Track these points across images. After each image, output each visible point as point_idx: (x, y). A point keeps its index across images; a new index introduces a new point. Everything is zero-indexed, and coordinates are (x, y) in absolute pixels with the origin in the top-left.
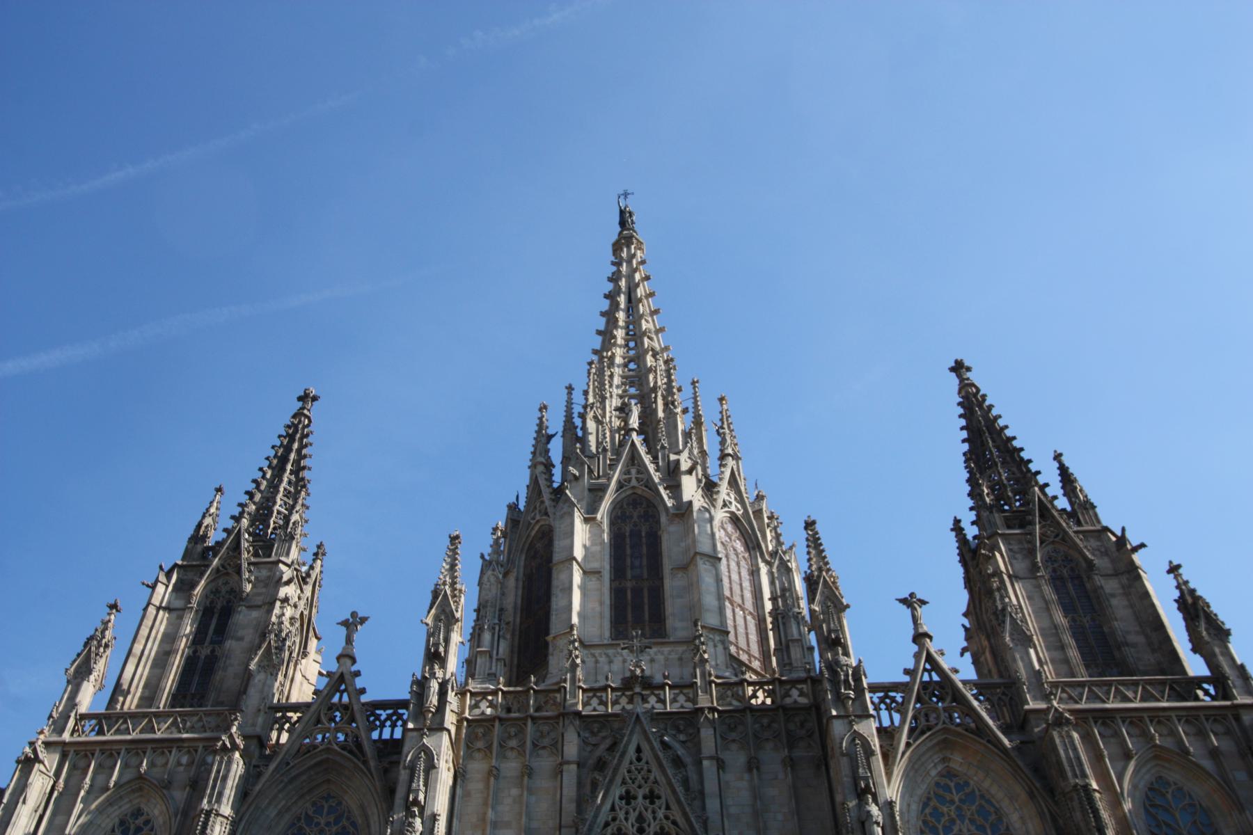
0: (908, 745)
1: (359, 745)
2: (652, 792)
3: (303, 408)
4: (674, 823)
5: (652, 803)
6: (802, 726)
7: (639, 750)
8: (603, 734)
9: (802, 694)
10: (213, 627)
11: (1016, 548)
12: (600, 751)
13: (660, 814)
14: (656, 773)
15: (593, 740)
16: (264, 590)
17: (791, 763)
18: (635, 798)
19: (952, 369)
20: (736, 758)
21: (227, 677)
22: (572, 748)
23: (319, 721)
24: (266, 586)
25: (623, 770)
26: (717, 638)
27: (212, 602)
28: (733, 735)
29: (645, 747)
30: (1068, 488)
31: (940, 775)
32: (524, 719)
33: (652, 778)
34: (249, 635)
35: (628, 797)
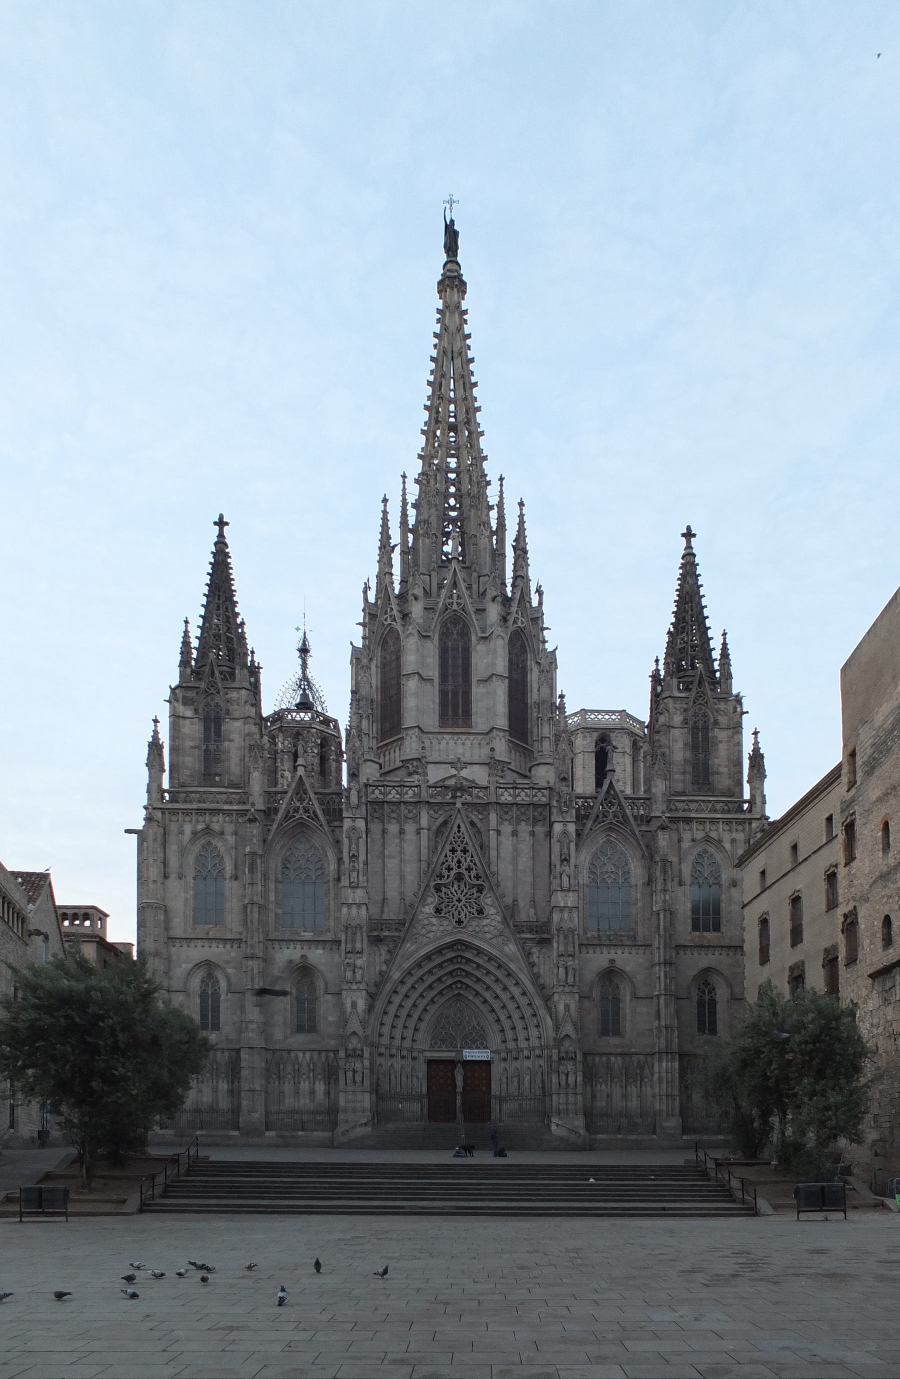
0: (591, 829)
1: (316, 816)
2: (465, 848)
3: (221, 535)
4: (475, 864)
6: (541, 814)
7: (459, 827)
8: (440, 812)
9: (544, 796)
11: (678, 706)
13: (468, 860)
14: (467, 839)
15: (436, 816)
19: (683, 535)
22: (424, 822)
23: (292, 800)
26: (501, 734)
28: (506, 817)
29: (462, 826)
30: (723, 661)
32: (400, 802)
35: (453, 851)
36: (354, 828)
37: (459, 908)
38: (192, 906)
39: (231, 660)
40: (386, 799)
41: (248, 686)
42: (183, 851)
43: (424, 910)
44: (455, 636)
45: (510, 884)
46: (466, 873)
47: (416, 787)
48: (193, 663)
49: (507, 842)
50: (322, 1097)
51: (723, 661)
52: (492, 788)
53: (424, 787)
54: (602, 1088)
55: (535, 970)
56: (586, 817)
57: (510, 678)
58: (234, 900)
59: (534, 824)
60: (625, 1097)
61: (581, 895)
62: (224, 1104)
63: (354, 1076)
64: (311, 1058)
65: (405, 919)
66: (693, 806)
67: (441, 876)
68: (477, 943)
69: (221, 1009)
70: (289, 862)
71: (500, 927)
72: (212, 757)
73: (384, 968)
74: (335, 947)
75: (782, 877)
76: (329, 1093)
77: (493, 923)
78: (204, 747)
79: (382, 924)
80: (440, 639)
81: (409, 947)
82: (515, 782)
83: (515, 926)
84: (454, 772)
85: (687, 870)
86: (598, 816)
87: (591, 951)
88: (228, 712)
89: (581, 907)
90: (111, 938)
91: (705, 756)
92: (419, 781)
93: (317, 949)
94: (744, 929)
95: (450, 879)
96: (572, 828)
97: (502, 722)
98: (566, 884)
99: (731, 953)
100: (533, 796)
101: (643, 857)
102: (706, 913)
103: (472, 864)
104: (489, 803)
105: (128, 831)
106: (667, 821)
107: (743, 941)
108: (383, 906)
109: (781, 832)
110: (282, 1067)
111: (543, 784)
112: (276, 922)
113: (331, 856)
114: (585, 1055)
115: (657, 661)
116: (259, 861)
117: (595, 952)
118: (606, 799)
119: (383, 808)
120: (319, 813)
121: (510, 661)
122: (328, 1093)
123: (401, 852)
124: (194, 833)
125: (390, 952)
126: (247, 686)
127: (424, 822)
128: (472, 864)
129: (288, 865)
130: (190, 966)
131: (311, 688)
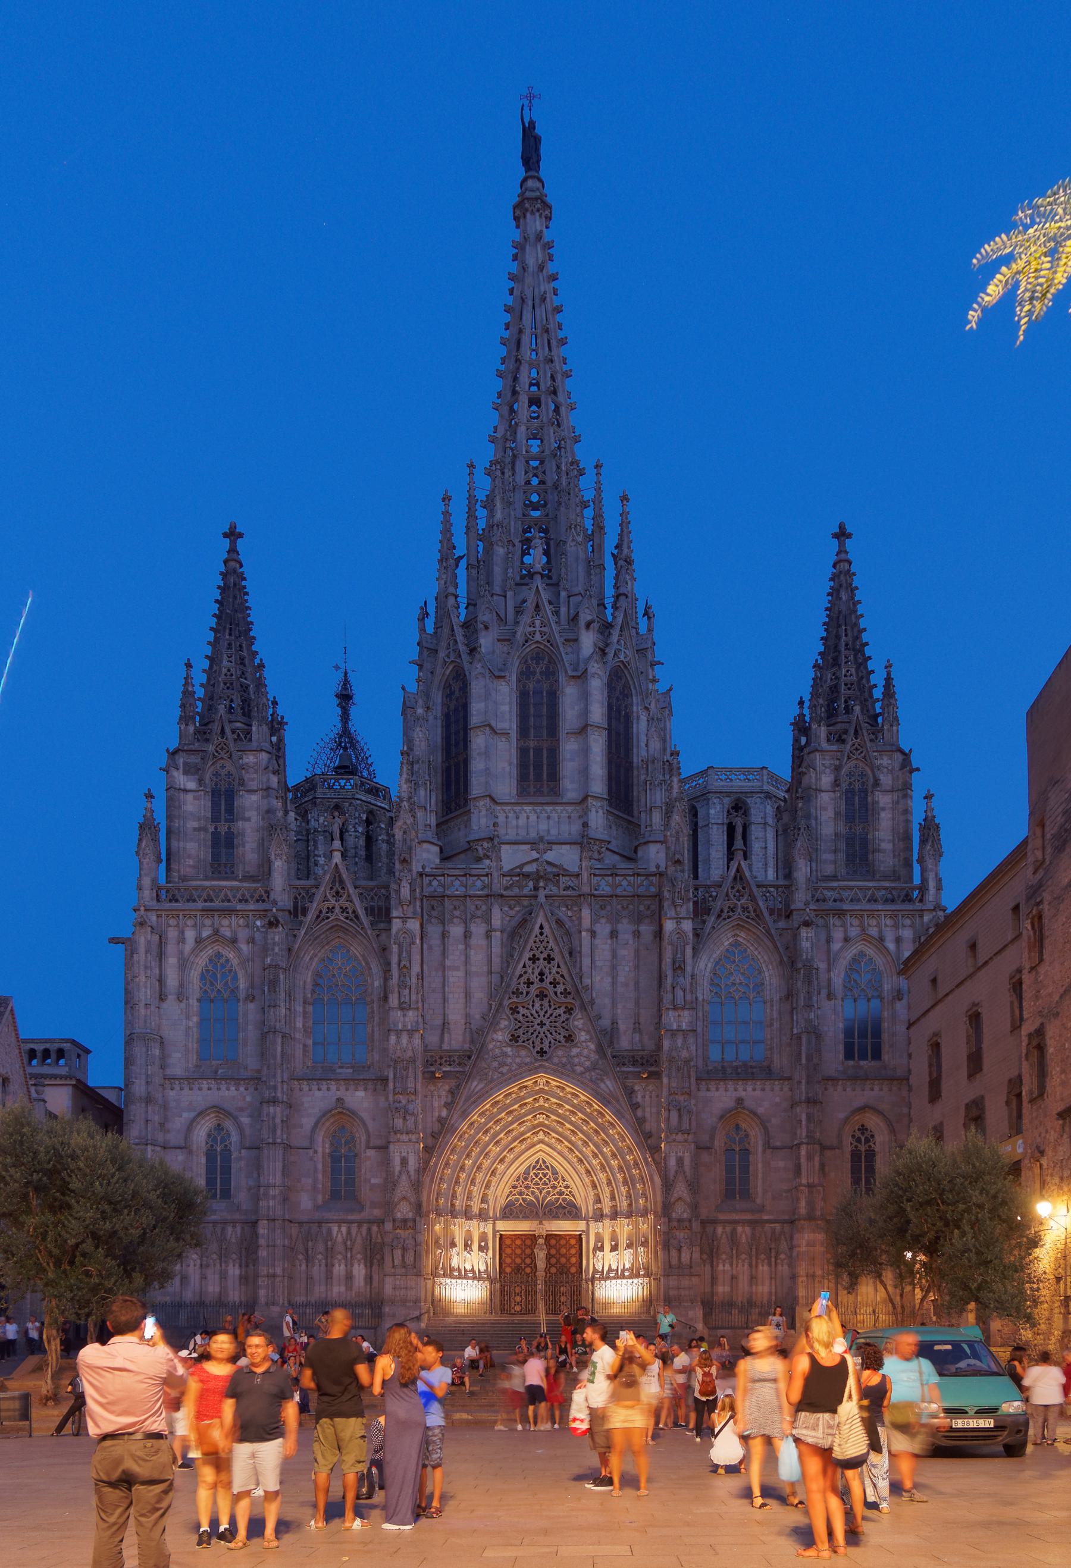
1: (357, 917)
2: (549, 956)
4: (562, 976)
5: (549, 963)
7: (541, 927)
8: (517, 909)
10: (223, 807)
12: (514, 923)
13: (554, 970)
14: (552, 944)
16: (255, 776)
17: (637, 934)
18: (538, 959)
20: (603, 929)
21: (248, 851)
24: (256, 772)
25: (531, 941)
27: (216, 785)
28: (603, 912)
31: (731, 945)
32: (466, 896)
34: (253, 814)
35: (534, 959)
36: (406, 932)
37: (542, 1035)
38: (195, 1037)
39: (247, 714)
40: (448, 893)
41: (269, 749)
42: (184, 965)
43: (495, 1036)
44: (538, 676)
45: (607, 1001)
46: (550, 988)
47: (487, 875)
48: (198, 718)
49: (604, 947)
50: (362, 1283)
51: (886, 702)
52: (585, 875)
53: (495, 874)
54: (723, 1267)
56: (708, 911)
57: (609, 730)
58: (250, 1027)
59: (639, 921)
60: (753, 1278)
61: (700, 1014)
62: (235, 1295)
63: (403, 1256)
64: (349, 1233)
65: (471, 1050)
66: (845, 894)
67: (517, 993)
69: (233, 1171)
70: (321, 977)
71: (594, 1057)
72: (223, 845)
73: (444, 1113)
74: (379, 1087)
75: (958, 986)
76: (371, 1278)
78: (211, 829)
79: (441, 1058)
80: (519, 681)
82: (614, 867)
83: (614, 1057)
84: (535, 855)
85: (838, 978)
86: (722, 911)
87: (712, 1087)
88: (243, 785)
89: (699, 1030)
90: (93, 1081)
91: (863, 828)
92: (490, 867)
94: (910, 1056)
95: (530, 996)
96: (687, 926)
97: (598, 786)
98: (679, 1000)
99: (894, 1088)
100: (638, 887)
101: (781, 962)
102: (863, 1035)
103: (558, 977)
104: (580, 896)
105: (114, 941)
106: (813, 914)
107: (909, 1071)
108: (442, 1034)
109: (957, 926)
110: (310, 1244)
111: (653, 869)
112: (304, 1055)
113: (376, 968)
114: (703, 1223)
115: (801, 703)
116: (282, 977)
117: (717, 1089)
118: (733, 888)
120: (361, 912)
121: (610, 707)
122: (369, 1278)
123: (467, 961)
124: (199, 941)
125: (452, 1093)
126: (269, 749)
127: (497, 921)
128: (558, 977)
129: (320, 981)
130: (192, 1115)
131: (354, 748)
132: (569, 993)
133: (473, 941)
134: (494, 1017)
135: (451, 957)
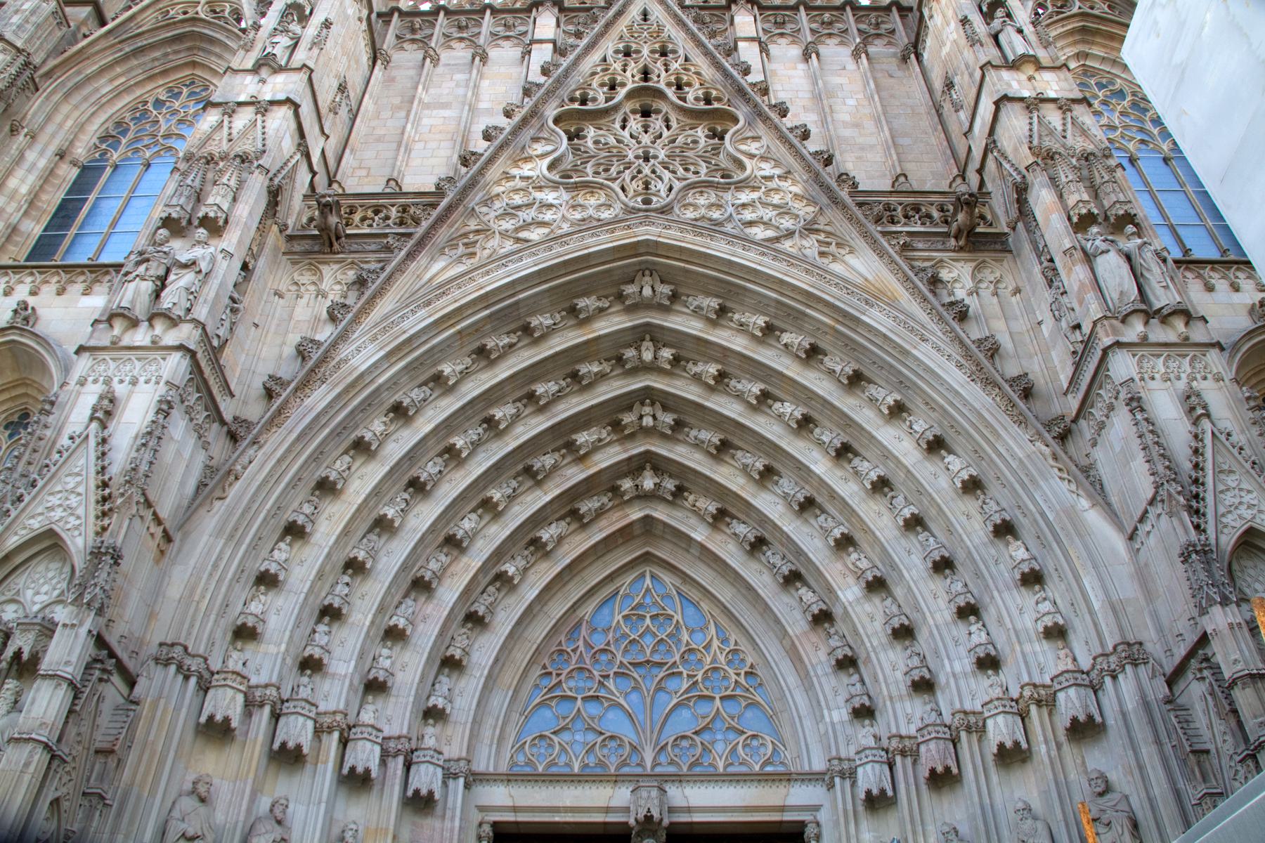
4: (698, 74)
7: (645, 15)
13: (675, 66)
14: (671, 30)
18: (638, 52)
25: (622, 26)
33: (665, 35)
43: (515, 171)
46: (671, 93)
55: (975, 332)
68: (719, 248)
71: (805, 211)
73: (325, 333)
77: (776, 199)
81: (436, 268)
83: (860, 205)
93: (87, 292)
119: (433, 25)
125: (361, 283)
132: (719, 99)
133: (490, 69)
134: (516, 131)
135: (432, 91)
